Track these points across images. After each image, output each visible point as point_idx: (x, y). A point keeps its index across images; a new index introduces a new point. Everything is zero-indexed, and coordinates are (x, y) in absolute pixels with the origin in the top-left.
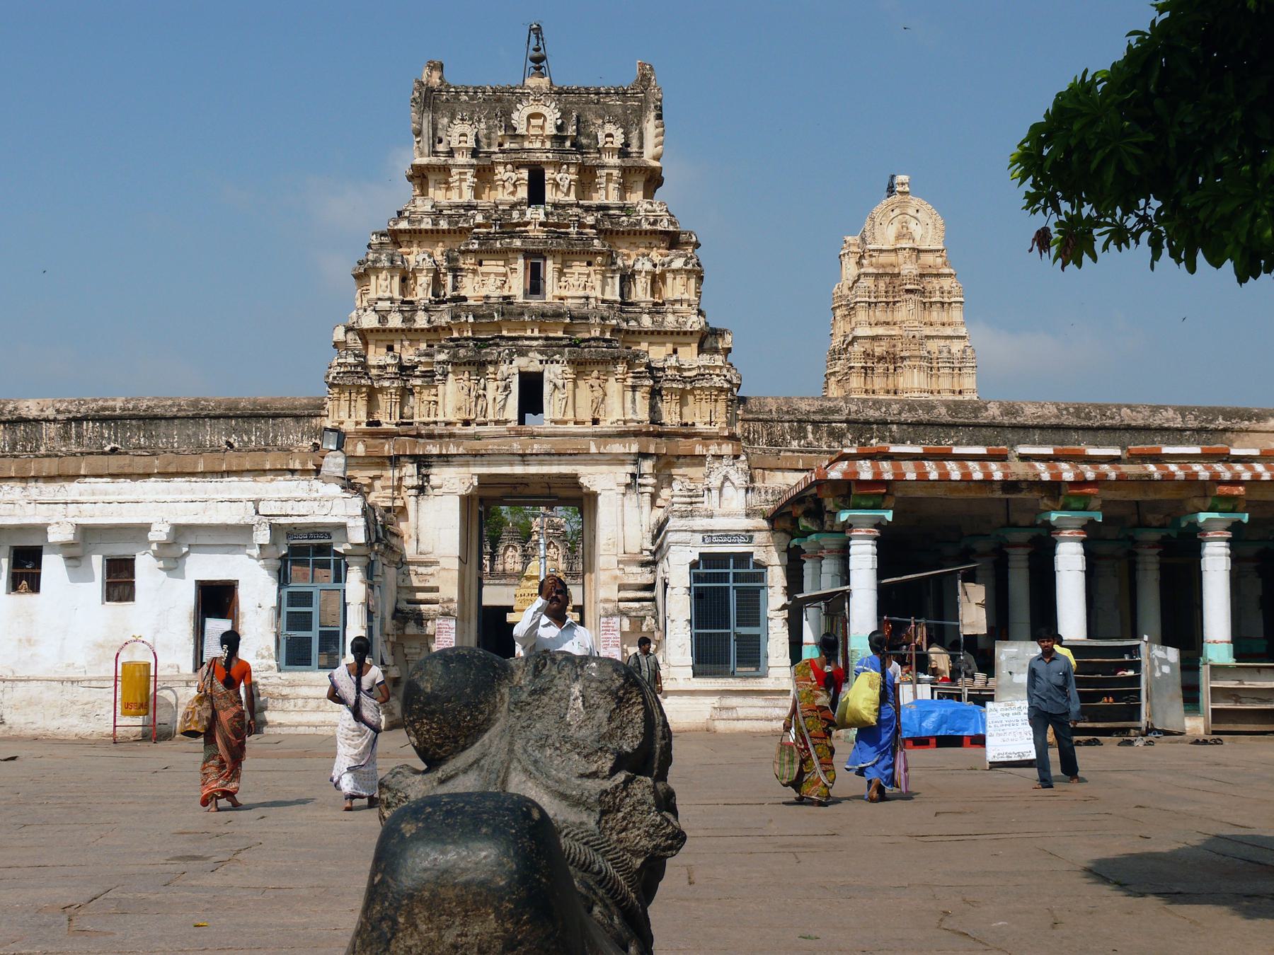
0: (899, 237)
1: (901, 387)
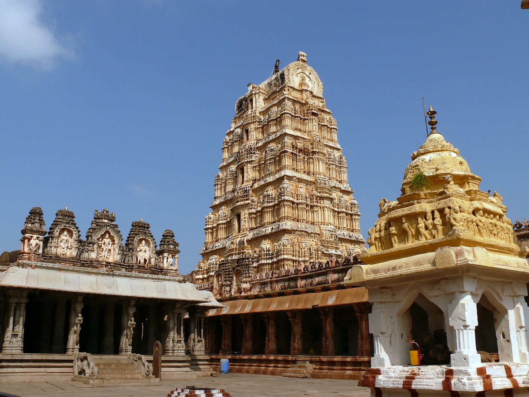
0: (301, 85)
1: (312, 170)
